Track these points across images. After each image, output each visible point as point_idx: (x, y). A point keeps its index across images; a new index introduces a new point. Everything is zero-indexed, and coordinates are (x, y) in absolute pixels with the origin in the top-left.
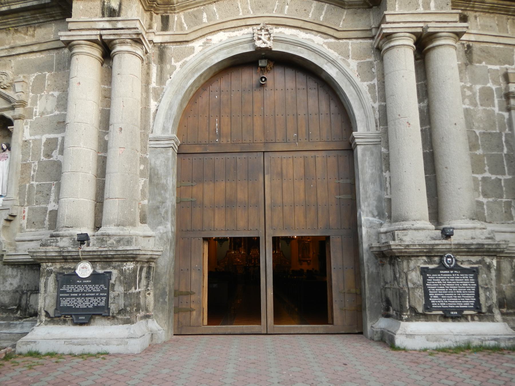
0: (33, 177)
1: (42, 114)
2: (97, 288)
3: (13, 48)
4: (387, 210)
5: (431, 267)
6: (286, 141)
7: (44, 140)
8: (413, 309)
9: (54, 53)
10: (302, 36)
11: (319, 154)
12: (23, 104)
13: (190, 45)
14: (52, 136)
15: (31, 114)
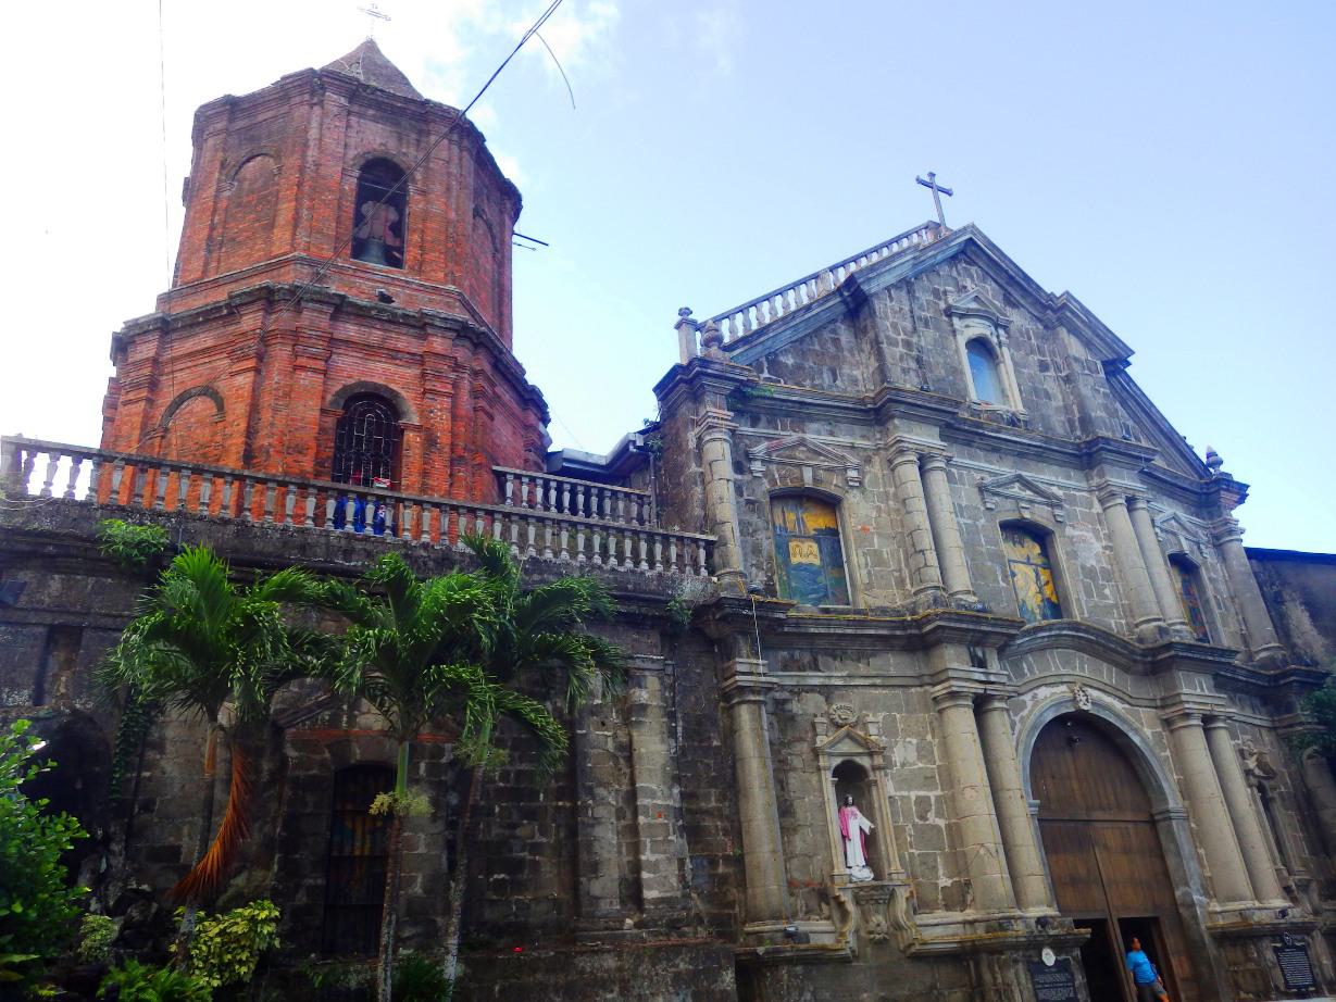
0: (911, 843)
1: (903, 765)
2: (1061, 977)
3: (850, 676)
4: (1209, 889)
5: (1279, 945)
6: (1102, 808)
7: (913, 798)
8: (1277, 988)
9: (899, 691)
10: (1107, 699)
11: (1130, 826)
12: (881, 751)
13: (1022, 698)
14: (922, 793)
15: (887, 765)
